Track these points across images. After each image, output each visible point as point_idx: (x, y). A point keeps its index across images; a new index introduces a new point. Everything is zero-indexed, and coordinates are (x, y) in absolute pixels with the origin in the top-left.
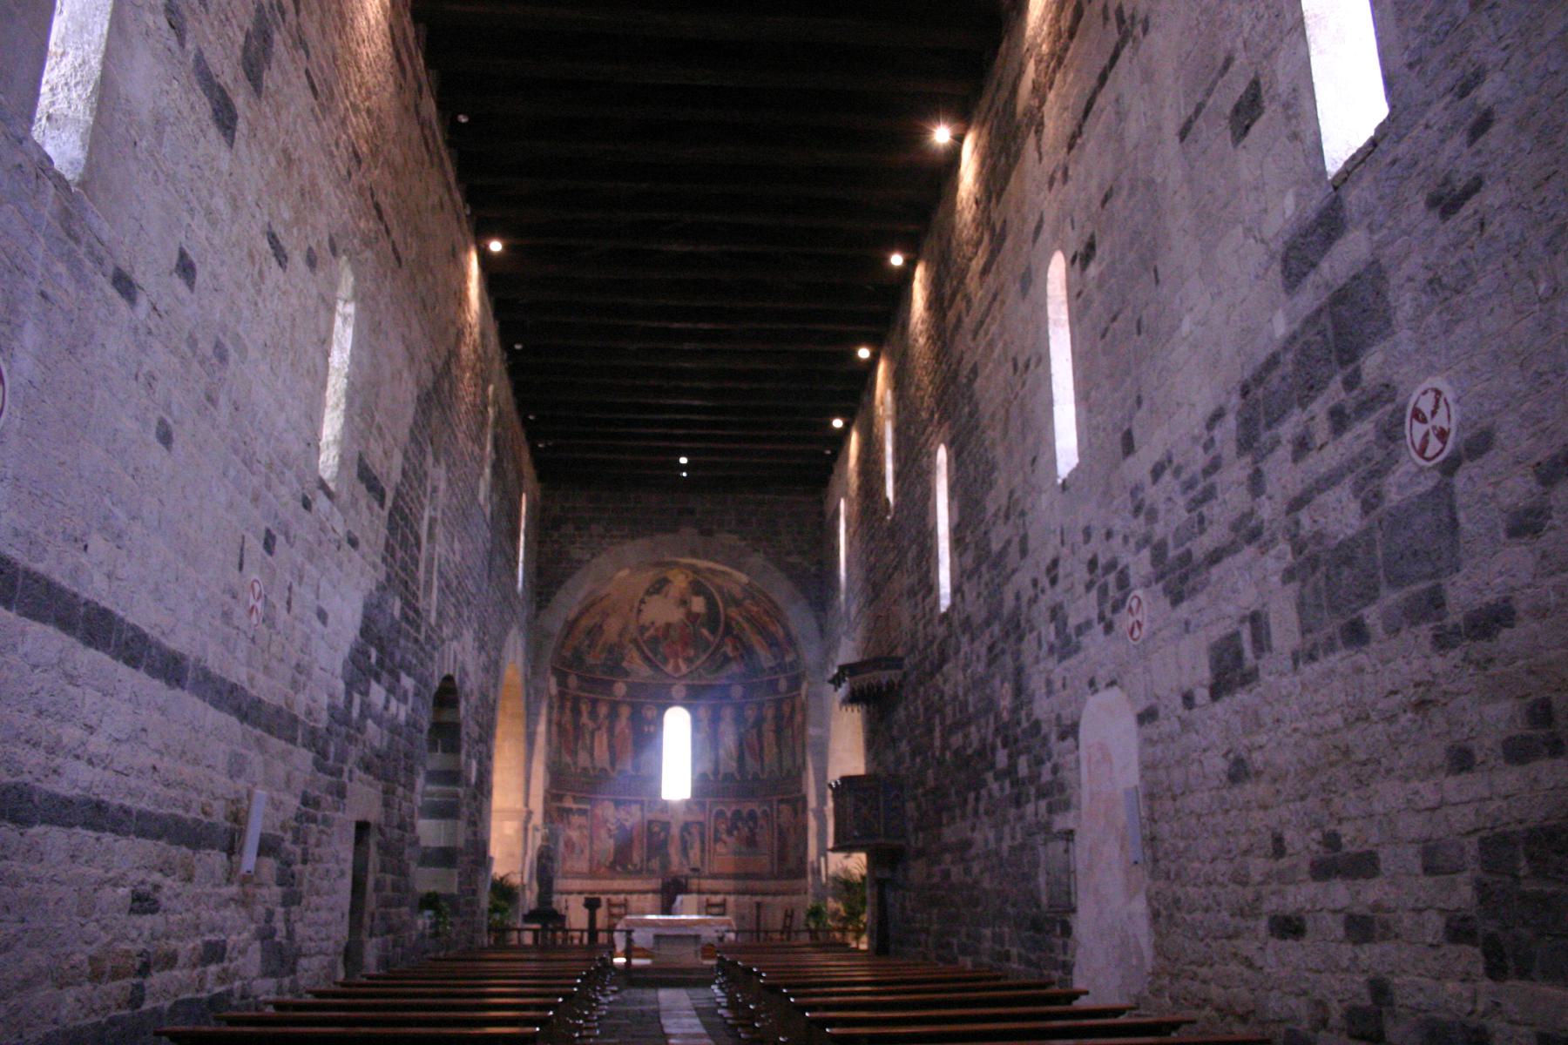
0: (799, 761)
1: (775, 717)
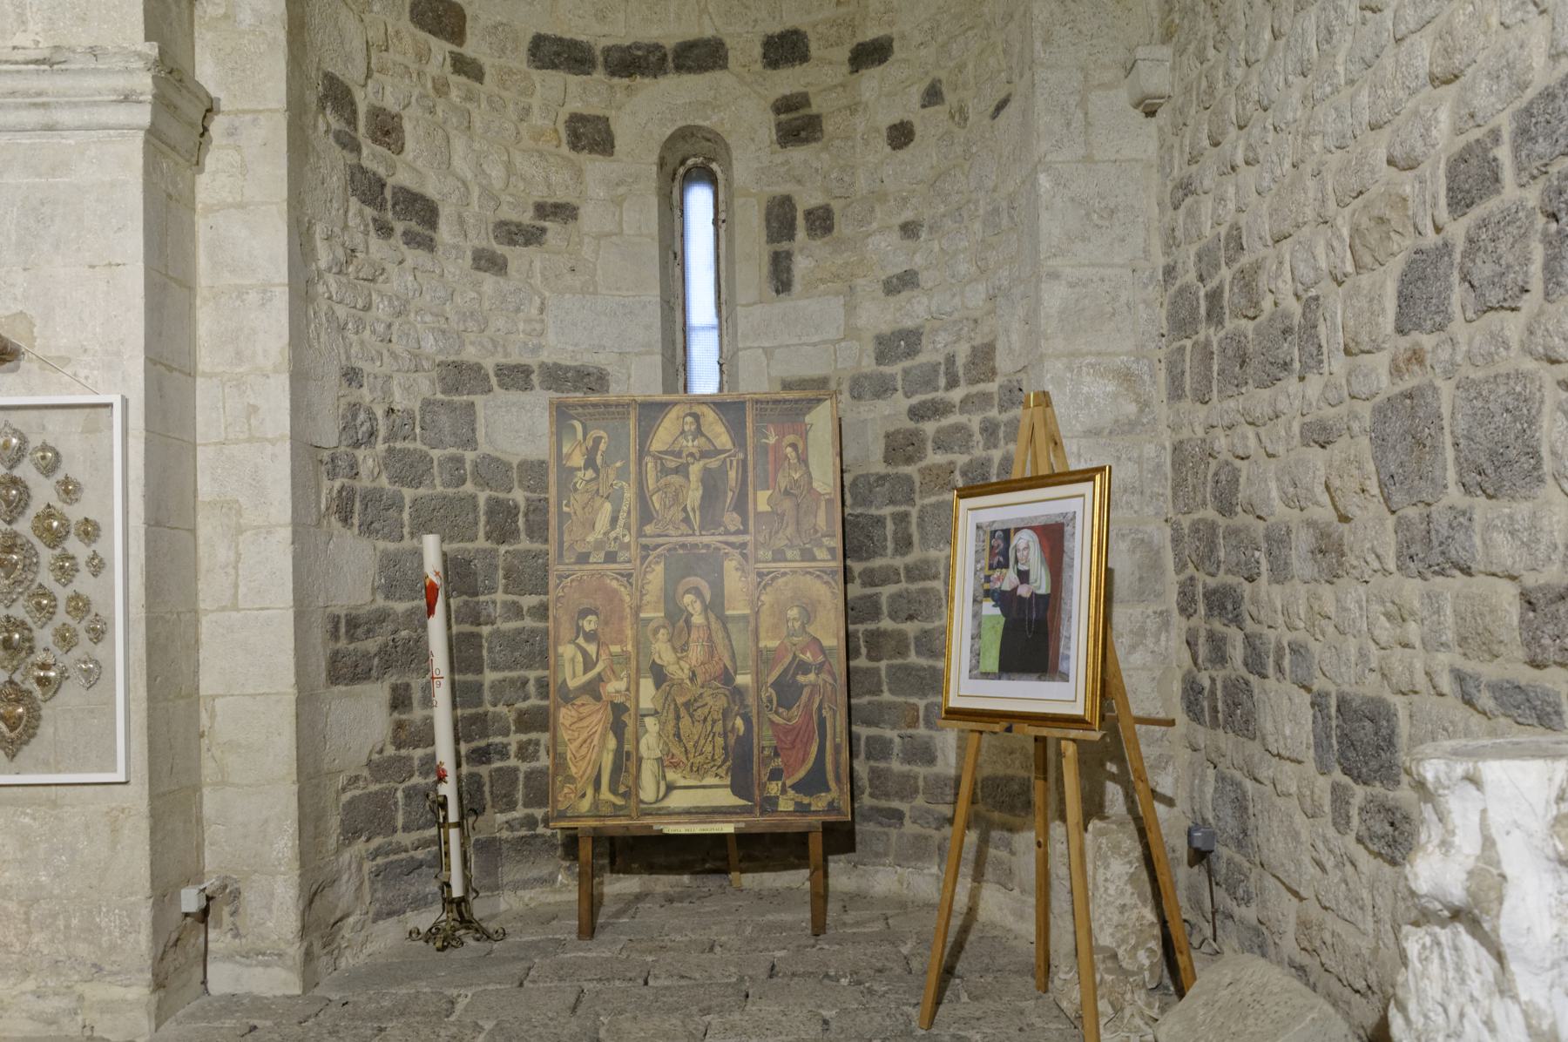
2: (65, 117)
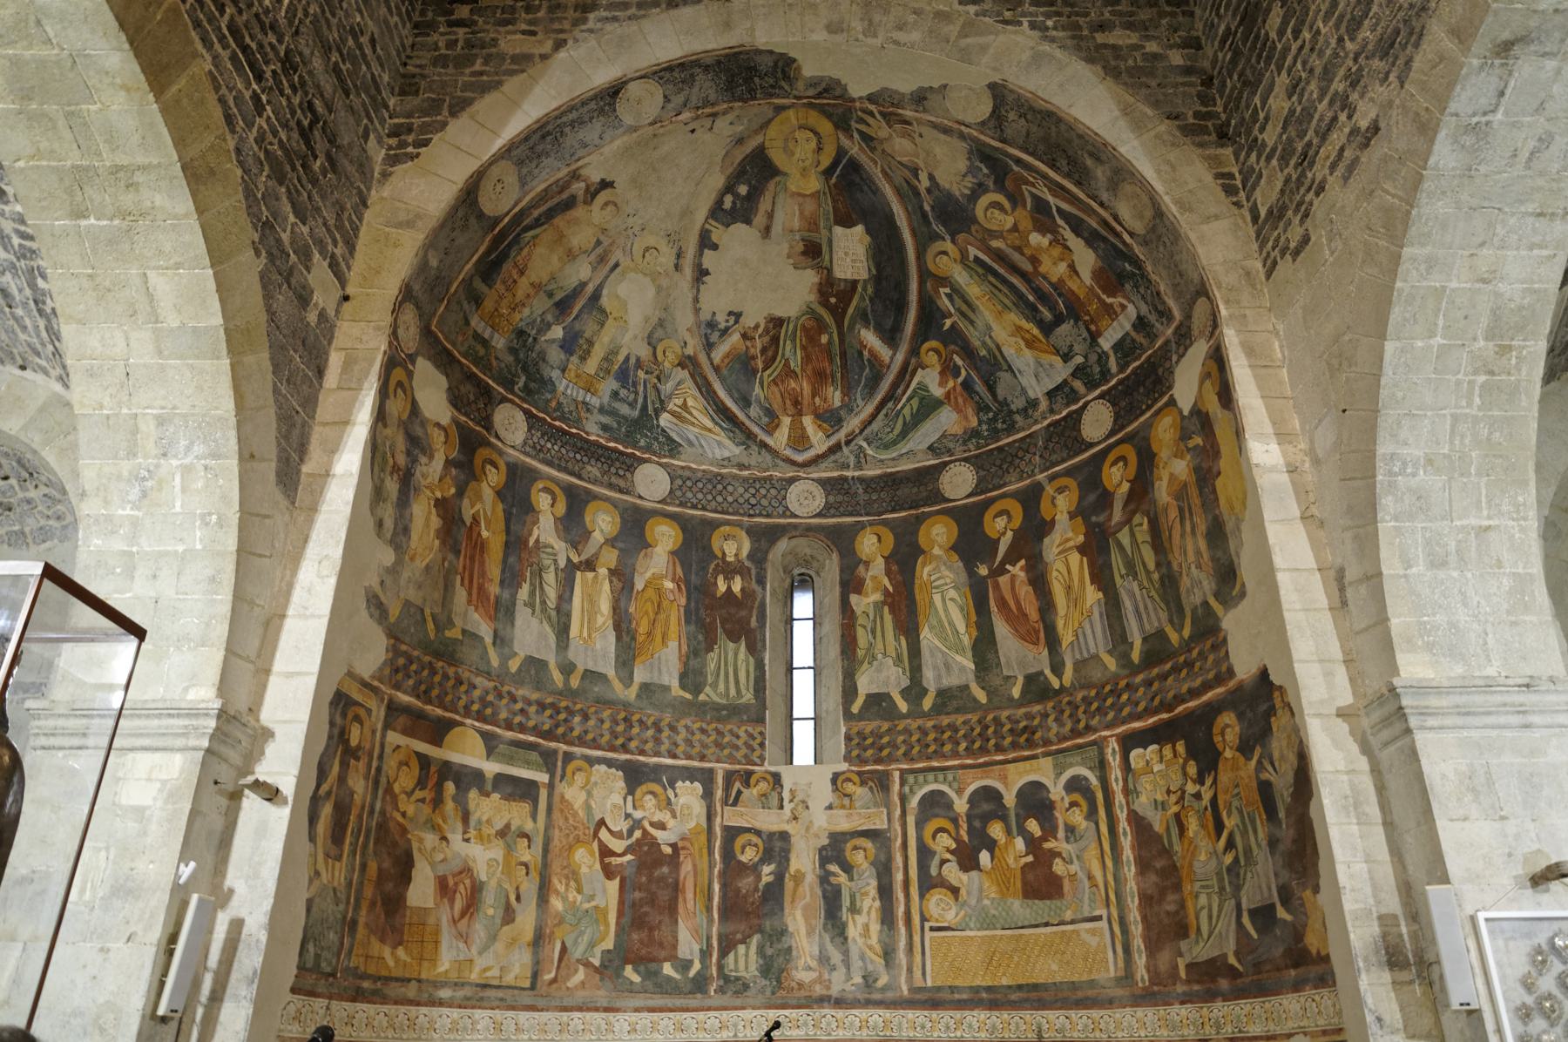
0: (1198, 585)
2: (1535, 719)
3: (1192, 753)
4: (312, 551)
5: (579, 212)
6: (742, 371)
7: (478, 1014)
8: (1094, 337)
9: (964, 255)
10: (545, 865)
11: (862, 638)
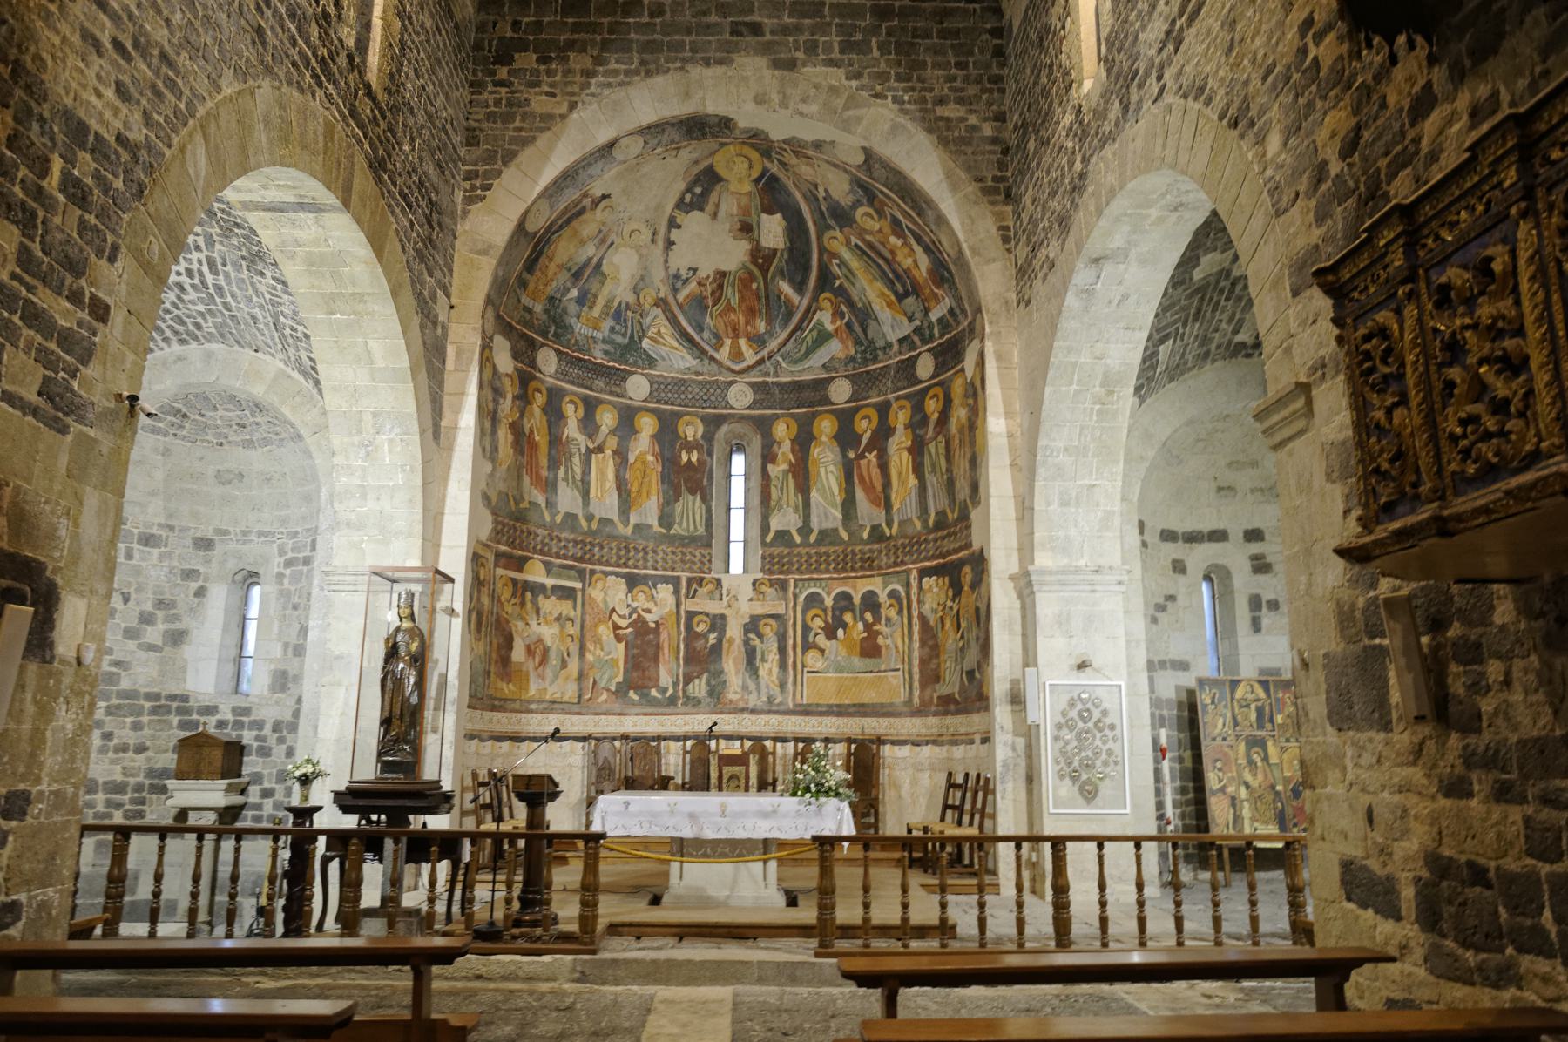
0: (963, 490)
1: (910, 426)
2: (1098, 588)
3: (951, 585)
4: (454, 475)
5: (587, 216)
6: (698, 307)
7: (551, 717)
8: (927, 311)
9: (848, 243)
10: (582, 636)
11: (774, 494)
